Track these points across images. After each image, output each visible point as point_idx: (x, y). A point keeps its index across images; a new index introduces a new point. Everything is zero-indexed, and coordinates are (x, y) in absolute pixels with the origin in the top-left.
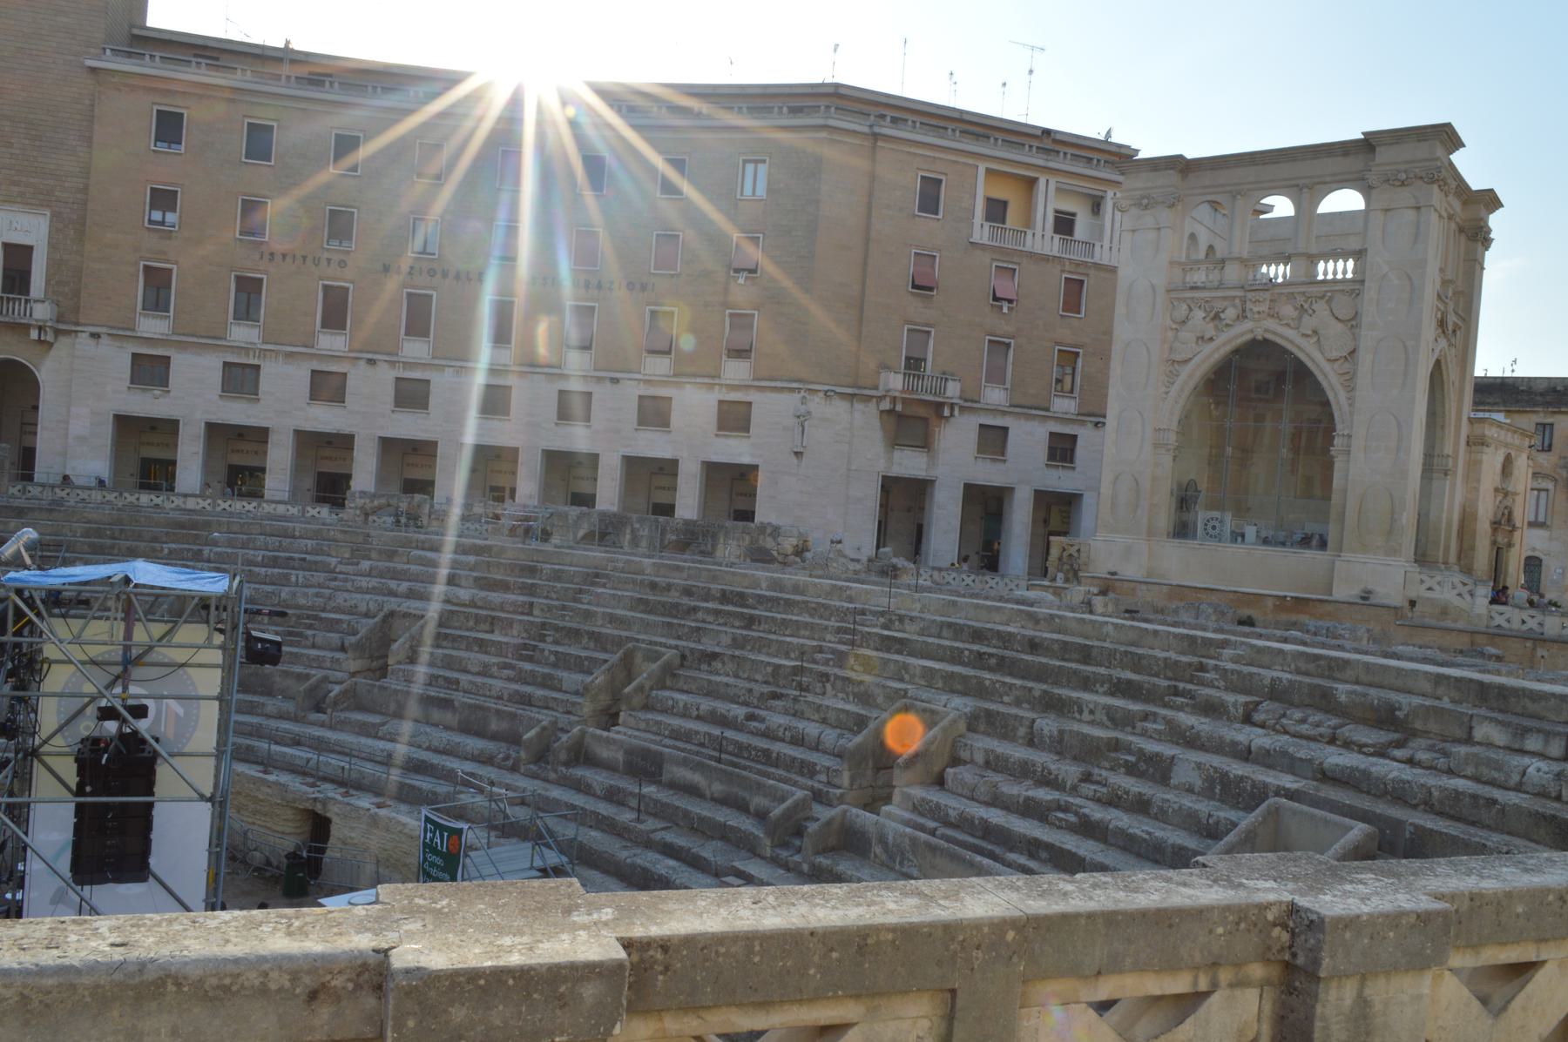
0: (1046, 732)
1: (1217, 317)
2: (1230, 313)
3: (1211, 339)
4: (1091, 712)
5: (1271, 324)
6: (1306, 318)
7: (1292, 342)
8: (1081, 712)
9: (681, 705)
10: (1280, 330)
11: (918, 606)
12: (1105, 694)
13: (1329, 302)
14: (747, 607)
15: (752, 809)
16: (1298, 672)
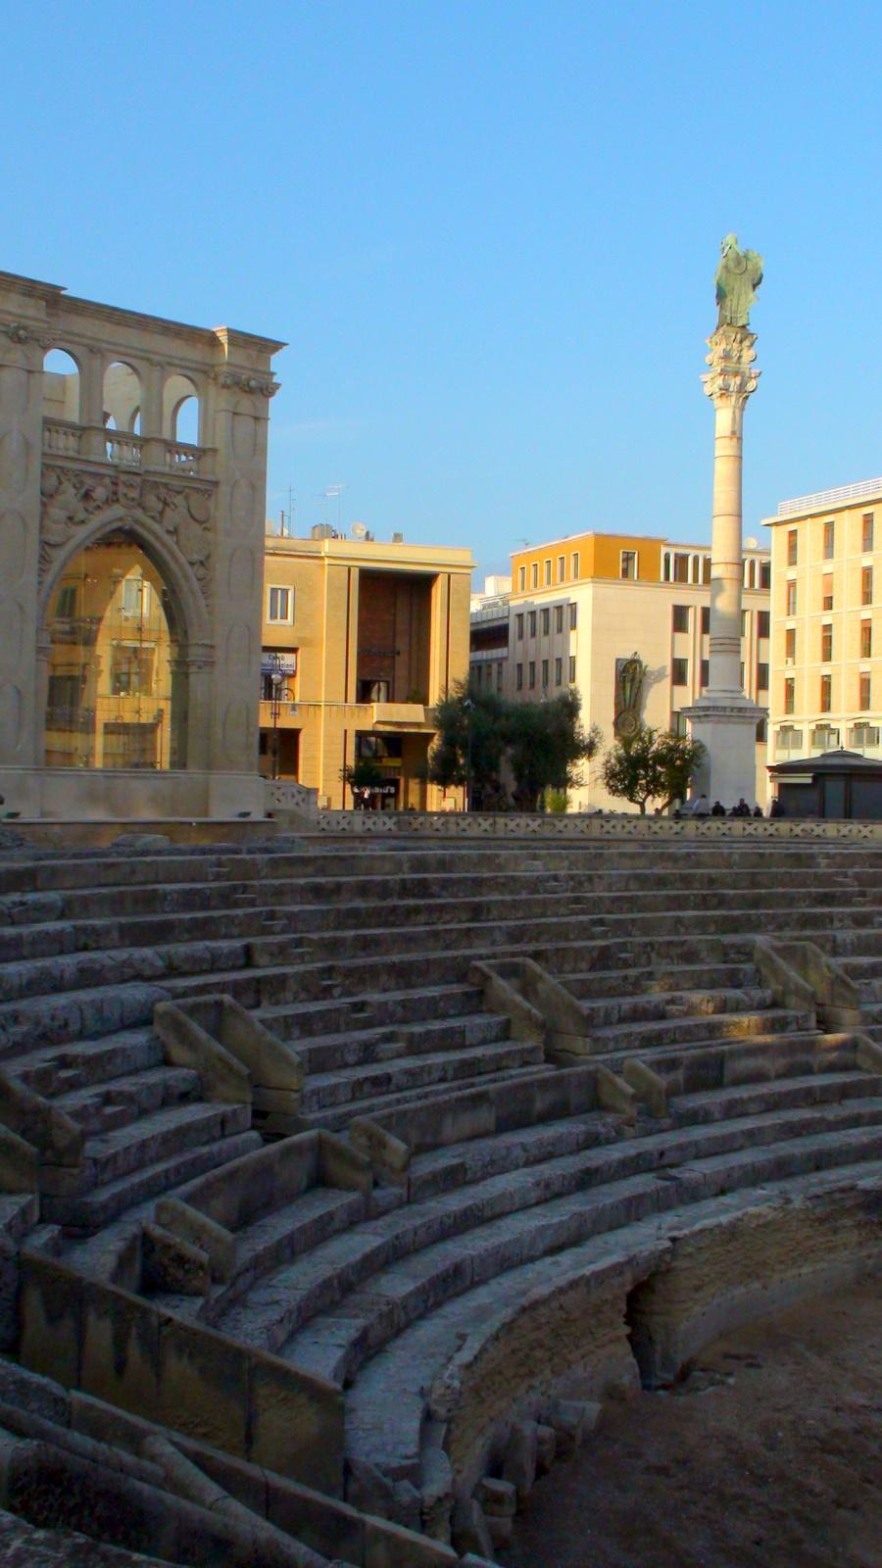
0: (848, 941)
1: (87, 496)
2: (100, 493)
3: (83, 522)
4: (841, 920)
5: (139, 513)
6: (168, 511)
7: (158, 538)
8: (832, 922)
9: (602, 1014)
10: (149, 522)
11: (566, 863)
12: (807, 906)
13: (187, 498)
14: (432, 896)
15: (815, 1068)
16: (871, 867)
